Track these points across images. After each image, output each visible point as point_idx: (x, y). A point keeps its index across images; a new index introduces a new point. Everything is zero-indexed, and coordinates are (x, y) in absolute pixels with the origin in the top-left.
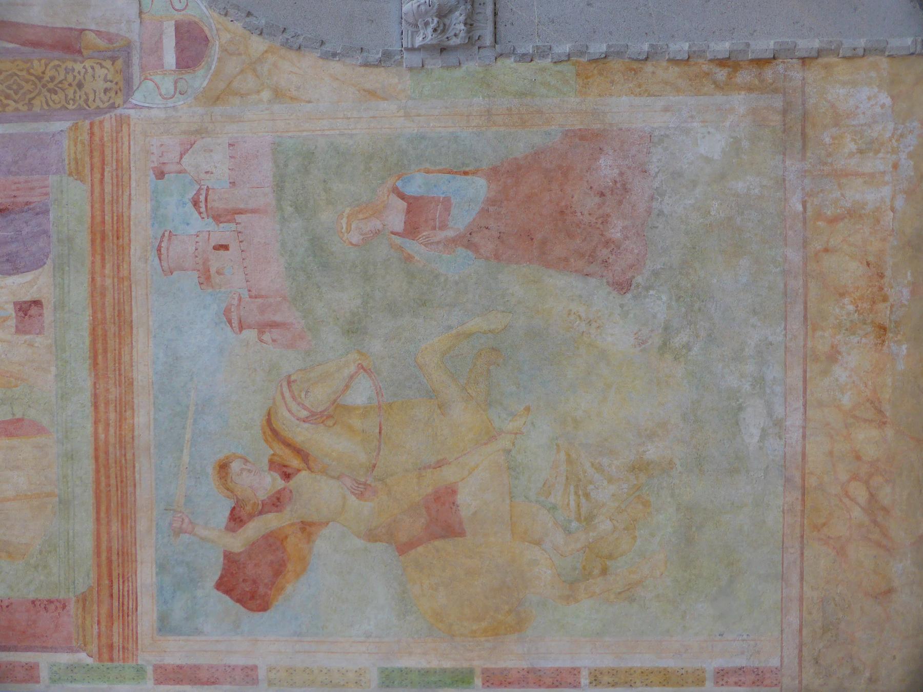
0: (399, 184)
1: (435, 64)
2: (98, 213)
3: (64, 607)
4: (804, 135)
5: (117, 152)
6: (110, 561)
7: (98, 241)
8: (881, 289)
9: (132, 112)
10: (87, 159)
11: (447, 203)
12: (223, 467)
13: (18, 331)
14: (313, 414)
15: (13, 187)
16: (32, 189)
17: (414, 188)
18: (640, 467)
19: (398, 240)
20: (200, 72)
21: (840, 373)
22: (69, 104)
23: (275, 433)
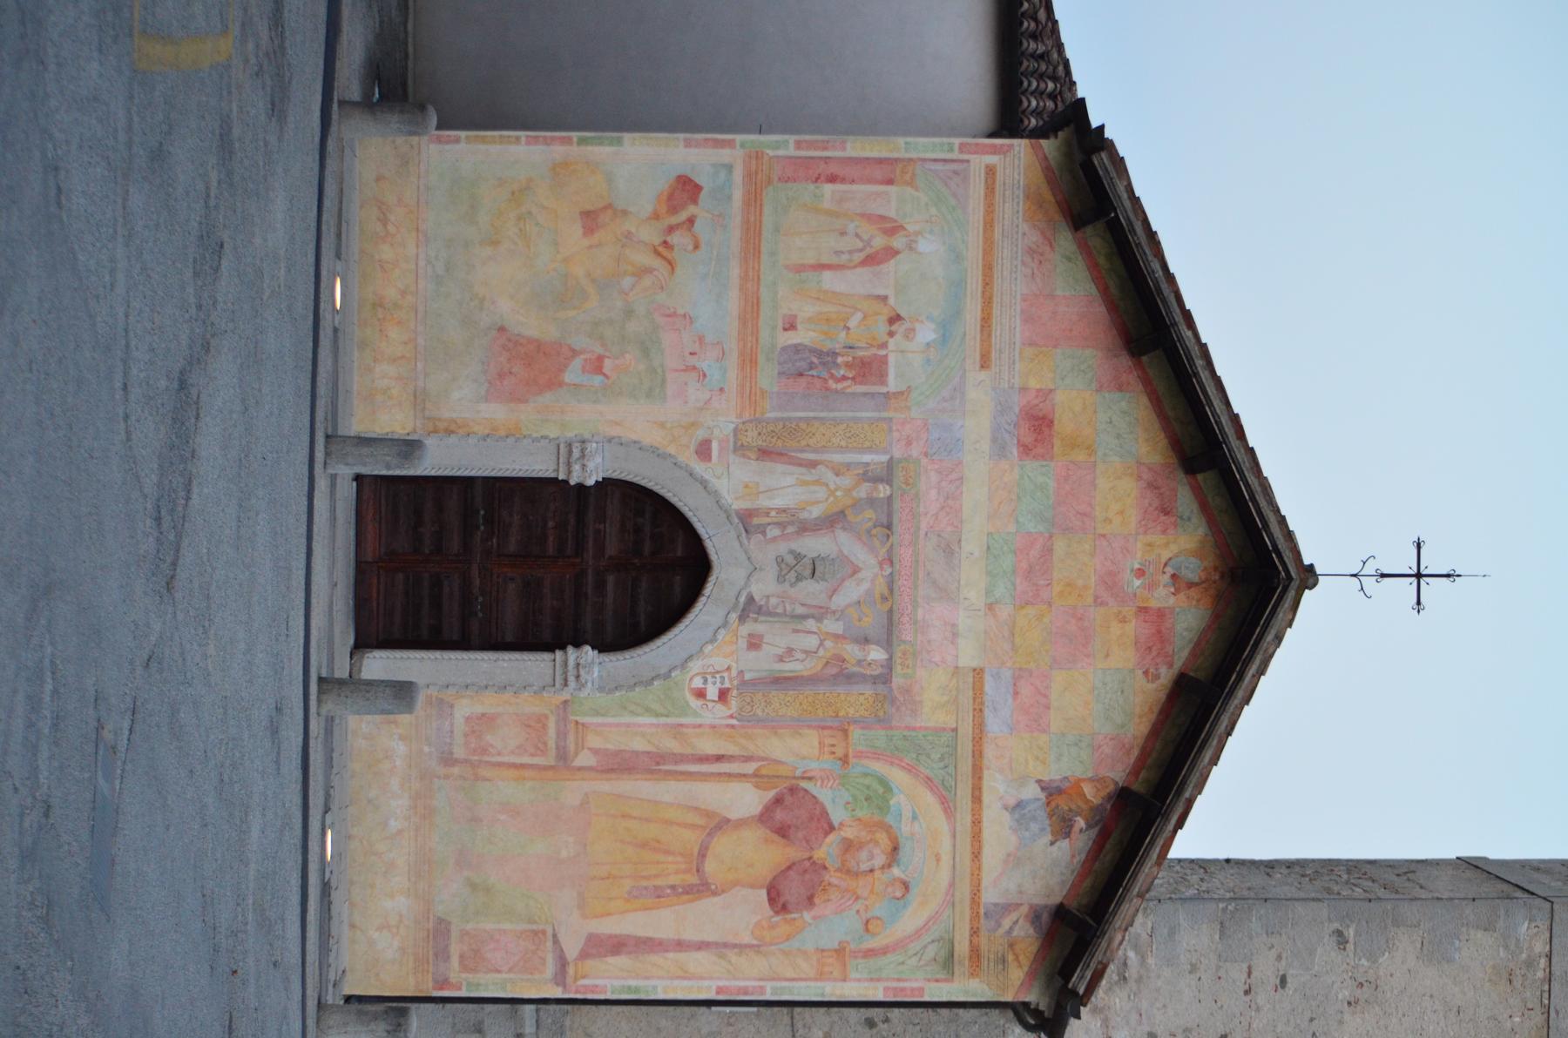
0: (606, 381)
1: (587, 436)
2: (753, 372)
3: (780, 179)
4: (415, 397)
6: (755, 201)
8: (381, 325)
9: (735, 420)
11: (584, 371)
12: (696, 247)
13: (795, 316)
14: (651, 272)
17: (597, 380)
18: (495, 243)
19: (607, 354)
20: (700, 438)
23: (670, 263)
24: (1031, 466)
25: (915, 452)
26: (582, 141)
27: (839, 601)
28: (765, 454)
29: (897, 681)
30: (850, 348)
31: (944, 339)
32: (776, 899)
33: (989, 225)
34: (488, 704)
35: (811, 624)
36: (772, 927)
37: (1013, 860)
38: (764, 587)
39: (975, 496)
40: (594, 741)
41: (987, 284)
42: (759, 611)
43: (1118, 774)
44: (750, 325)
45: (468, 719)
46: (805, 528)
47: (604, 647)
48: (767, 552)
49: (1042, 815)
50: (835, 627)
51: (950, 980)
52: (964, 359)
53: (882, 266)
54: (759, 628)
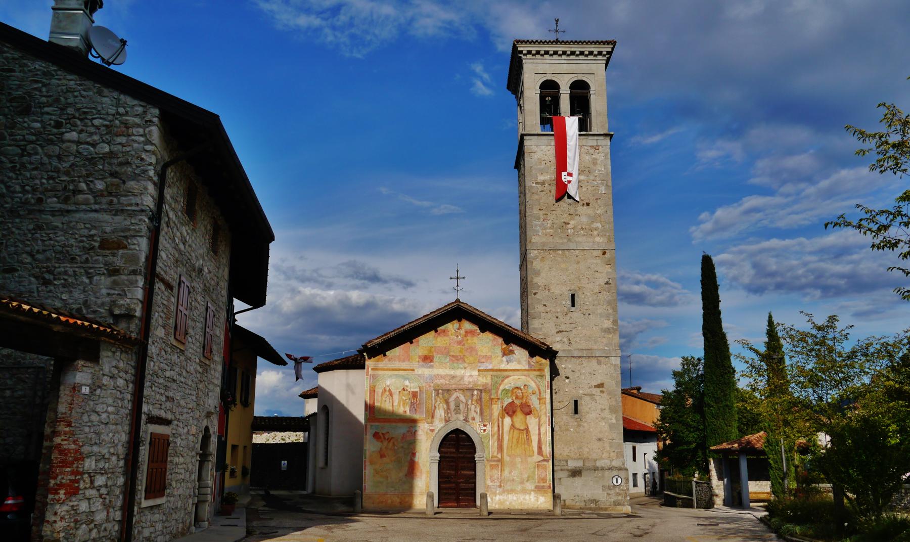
18: (387, 477)
21: (396, 498)
24: (435, 360)
25: (432, 385)
26: (365, 458)
27: (464, 401)
28: (433, 417)
29: (481, 388)
31: (408, 379)
32: (529, 413)
33: (383, 370)
34: (488, 477)
35: (469, 407)
36: (535, 414)
37: (519, 363)
38: (461, 417)
39: (441, 372)
40: (495, 454)
41: (396, 370)
42: (466, 418)
43: (500, 340)
45: (491, 482)
46: (448, 408)
47: (475, 452)
48: (454, 416)
49: (509, 356)
50: (470, 401)
51: (545, 375)
54: (470, 418)
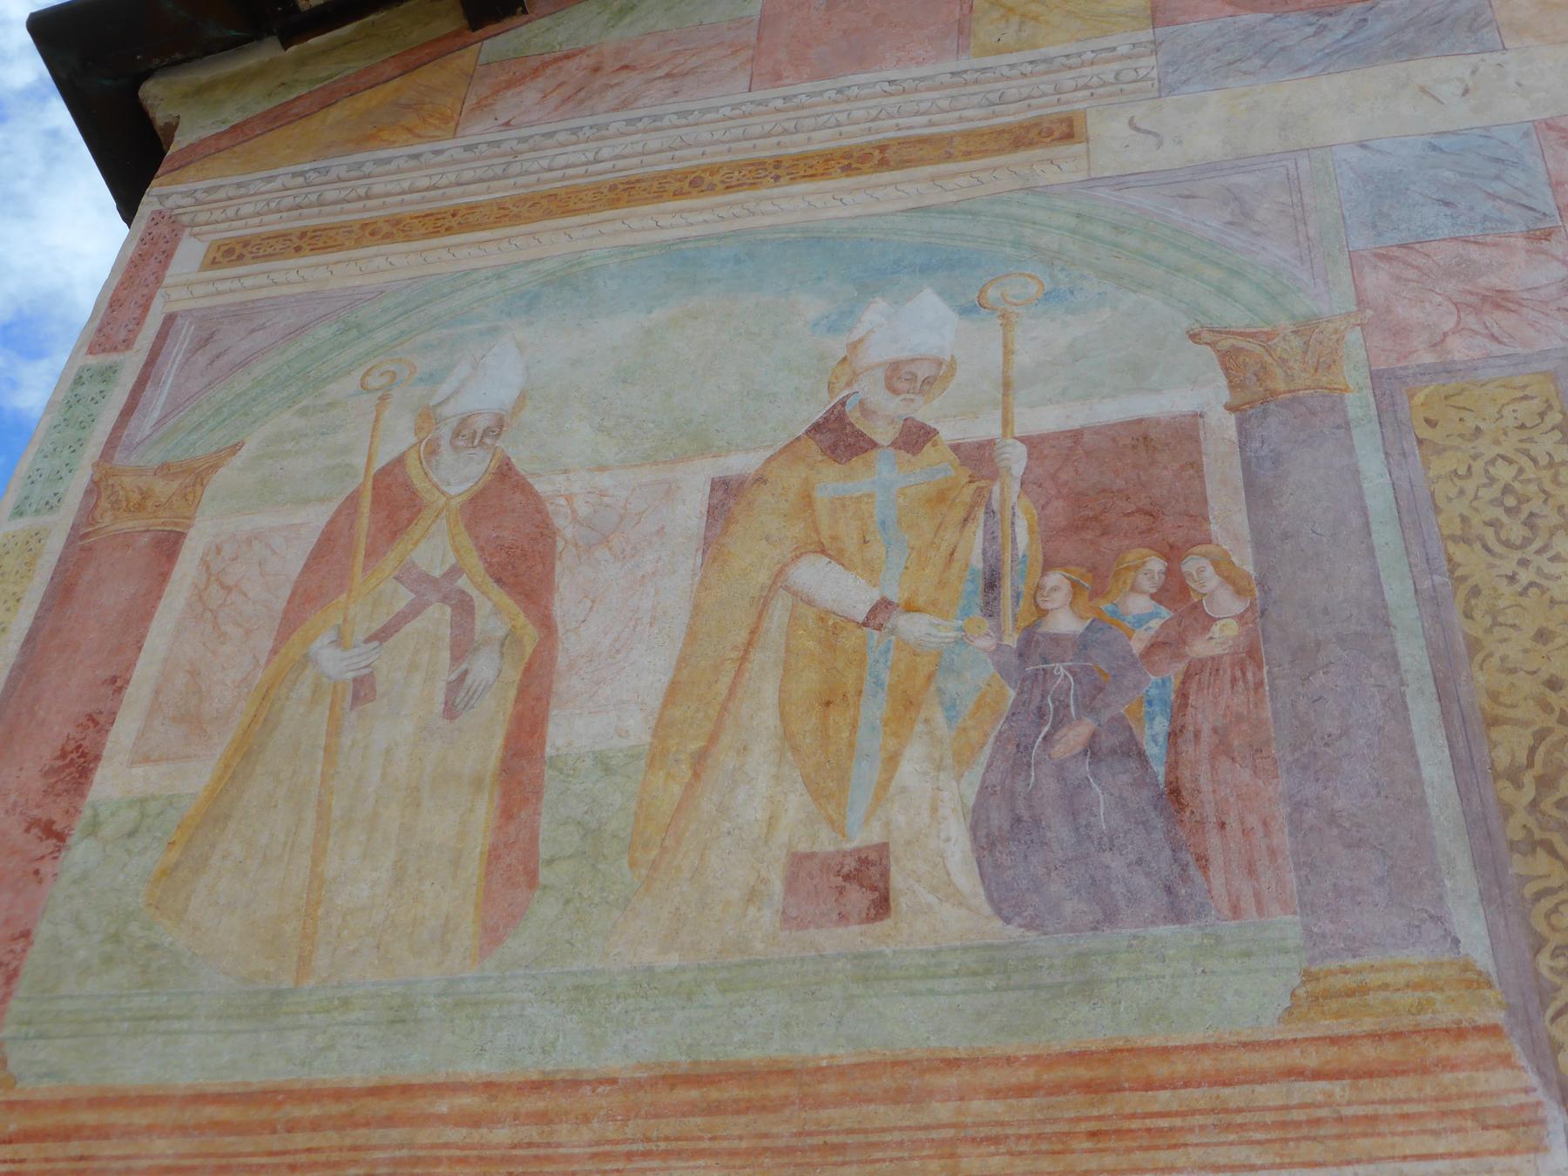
5: (1405, 1117)
7: (1083, 1073)
10: (1368, 1024)
13: (799, 862)
15: (1253, 820)
16: (1251, 871)
22: (1554, 956)
30: (992, 584)
33: (441, 223)
44: (846, 1116)
52: (1030, 190)
53: (559, 522)
